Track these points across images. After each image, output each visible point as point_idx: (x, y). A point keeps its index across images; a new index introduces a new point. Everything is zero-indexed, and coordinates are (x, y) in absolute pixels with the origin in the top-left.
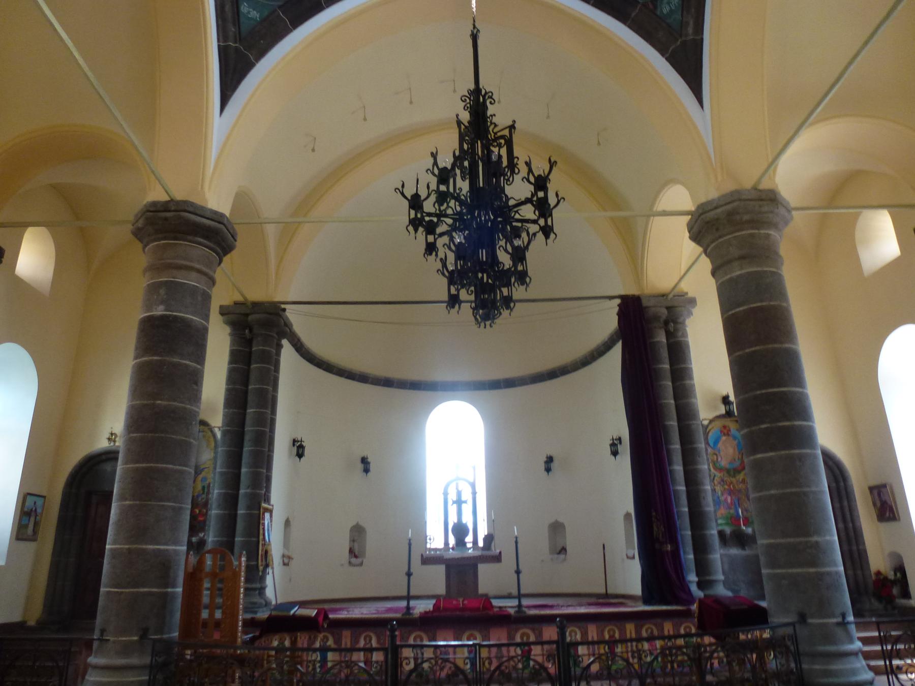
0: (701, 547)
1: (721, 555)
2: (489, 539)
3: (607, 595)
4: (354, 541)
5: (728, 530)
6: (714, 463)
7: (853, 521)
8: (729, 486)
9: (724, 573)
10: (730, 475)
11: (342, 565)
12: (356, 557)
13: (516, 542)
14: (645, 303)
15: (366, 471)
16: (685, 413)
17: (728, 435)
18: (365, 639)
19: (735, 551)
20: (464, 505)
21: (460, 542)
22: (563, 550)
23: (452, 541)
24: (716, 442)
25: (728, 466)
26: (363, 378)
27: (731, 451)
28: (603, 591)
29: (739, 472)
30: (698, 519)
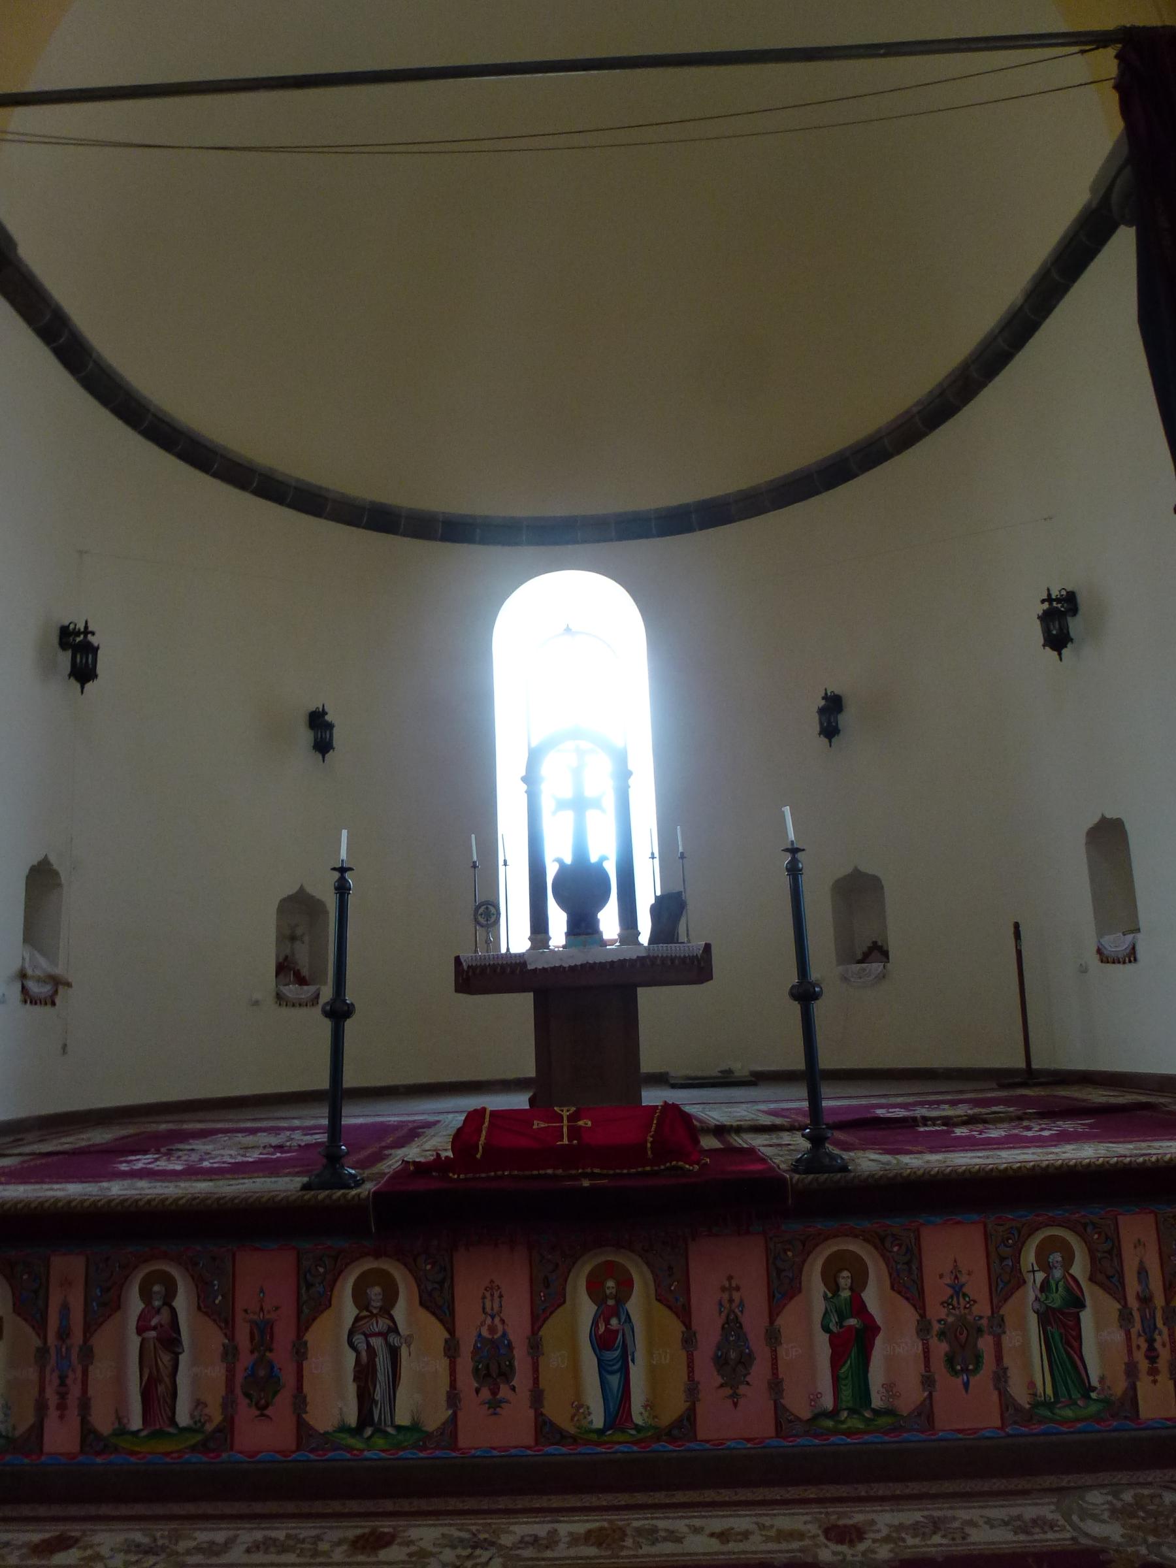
2: (669, 910)
3: (1029, 1076)
4: (293, 938)
11: (256, 1003)
12: (302, 981)
13: (794, 871)
15: (323, 746)
18: (146, 1294)
20: (591, 815)
21: (582, 925)
22: (878, 951)
23: (558, 921)
26: (308, 500)
28: (1022, 1065)
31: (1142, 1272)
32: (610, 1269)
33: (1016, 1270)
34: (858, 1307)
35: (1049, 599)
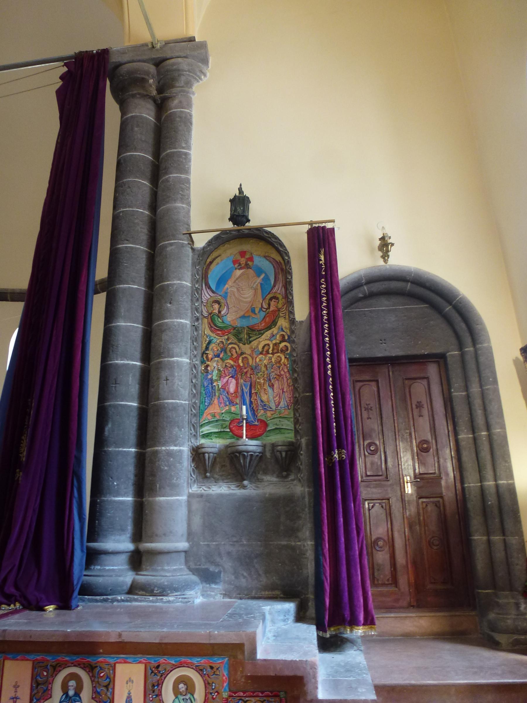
0: (146, 480)
1: (190, 496)
5: (214, 445)
6: (211, 317)
7: (488, 427)
8: (236, 360)
9: (190, 536)
10: (240, 340)
14: (114, 59)
16: (159, 230)
17: (247, 266)
19: (222, 489)
24: (222, 281)
25: (239, 324)
27: (248, 295)
29: (260, 333)
30: (149, 424)
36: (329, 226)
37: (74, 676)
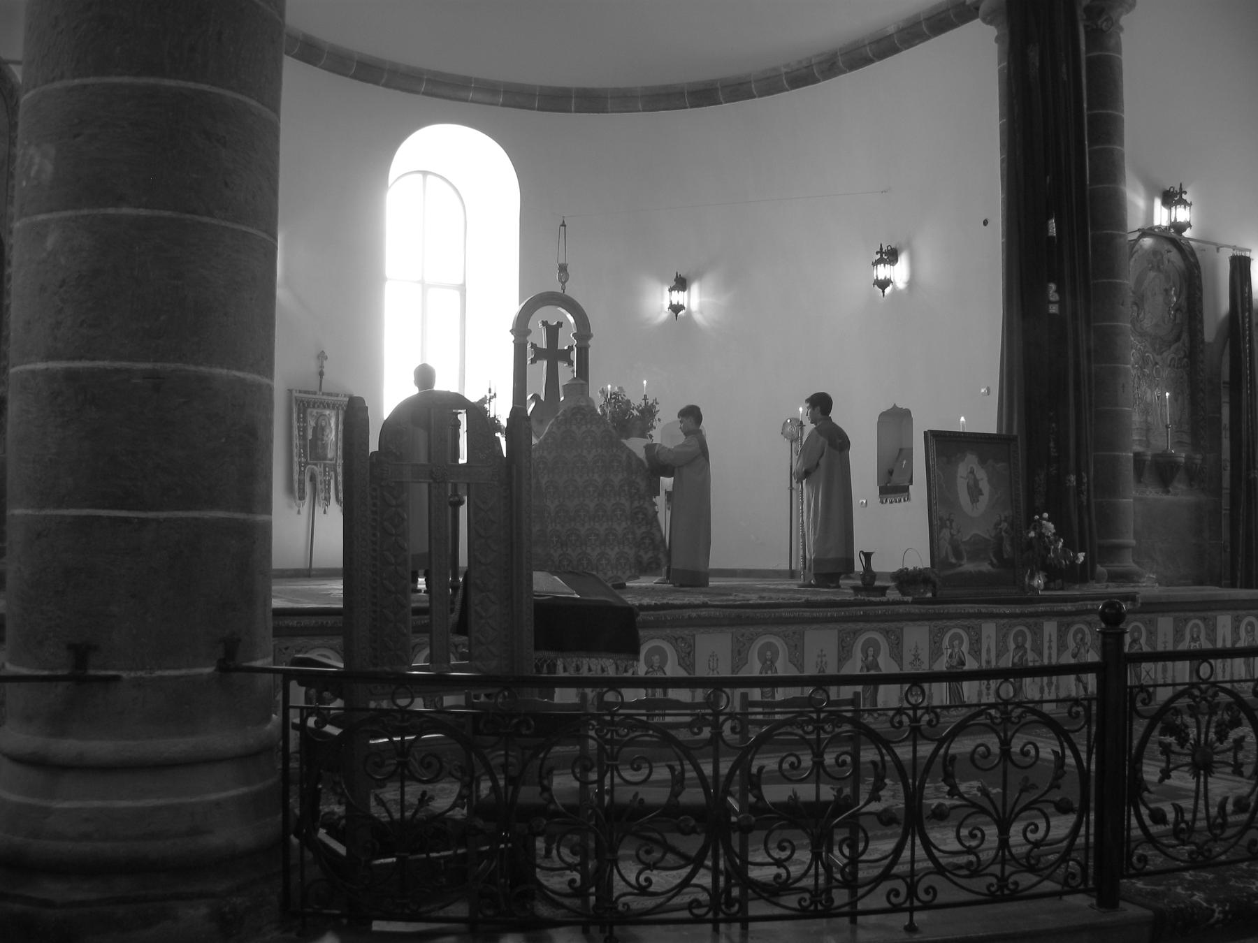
1: (1135, 499)
19: (1153, 494)
31: (988, 650)
32: (769, 646)
33: (940, 648)
34: (877, 665)
35: (881, 252)
36: (1248, 254)
37: (1197, 625)
